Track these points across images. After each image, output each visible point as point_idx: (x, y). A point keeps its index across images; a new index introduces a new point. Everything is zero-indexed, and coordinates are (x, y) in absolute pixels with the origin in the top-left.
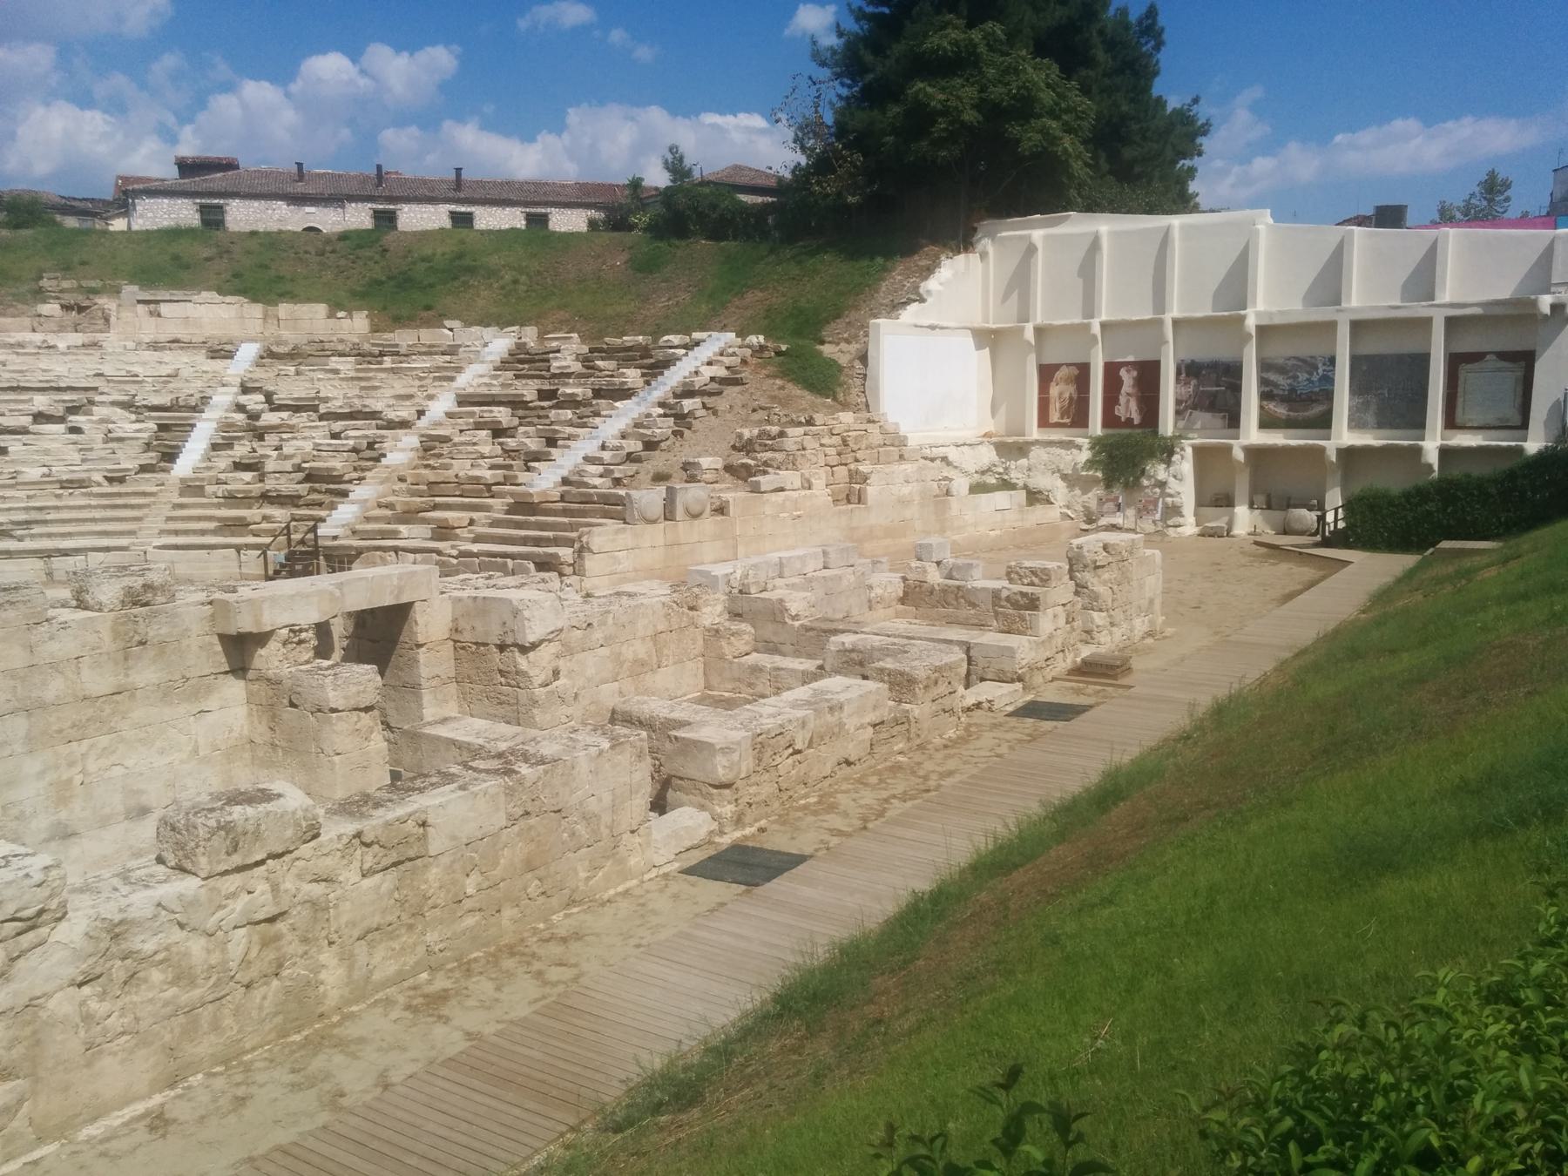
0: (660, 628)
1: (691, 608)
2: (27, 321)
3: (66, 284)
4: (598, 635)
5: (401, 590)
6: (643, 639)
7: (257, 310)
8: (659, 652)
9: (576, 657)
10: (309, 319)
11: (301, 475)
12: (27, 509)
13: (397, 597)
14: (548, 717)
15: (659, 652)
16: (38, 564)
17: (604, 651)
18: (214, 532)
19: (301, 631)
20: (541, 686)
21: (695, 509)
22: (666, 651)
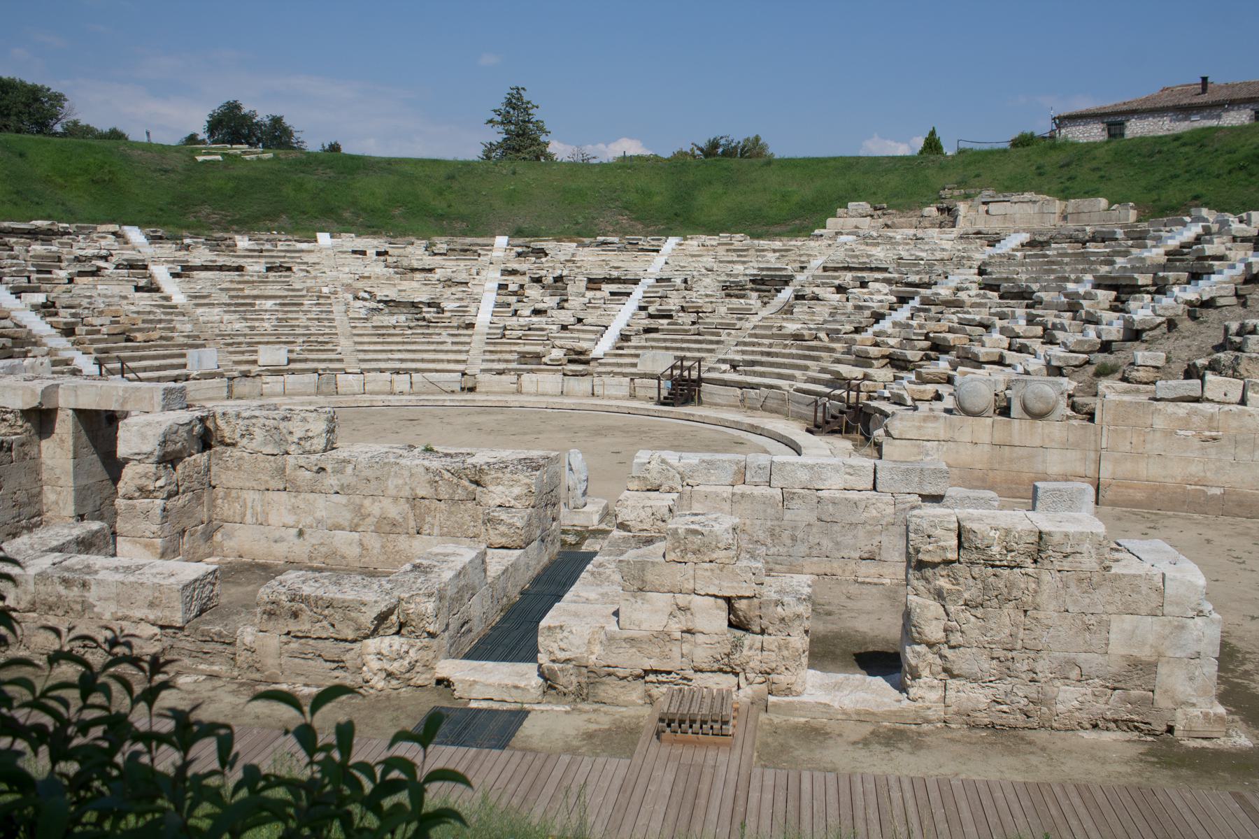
0: (421, 493)
1: (477, 483)
2: (914, 220)
3: (956, 193)
4: (331, 481)
5: (125, 401)
6: (396, 499)
7: (1058, 206)
8: (420, 518)
9: (303, 495)
10: (1096, 211)
11: (927, 344)
12: (762, 353)
13: (122, 405)
14: (129, 526)
15: (420, 518)
16: (738, 391)
17: (341, 499)
18: (826, 383)
19: (7, 412)
20: (124, 497)
21: (1037, 406)
22: (428, 519)
